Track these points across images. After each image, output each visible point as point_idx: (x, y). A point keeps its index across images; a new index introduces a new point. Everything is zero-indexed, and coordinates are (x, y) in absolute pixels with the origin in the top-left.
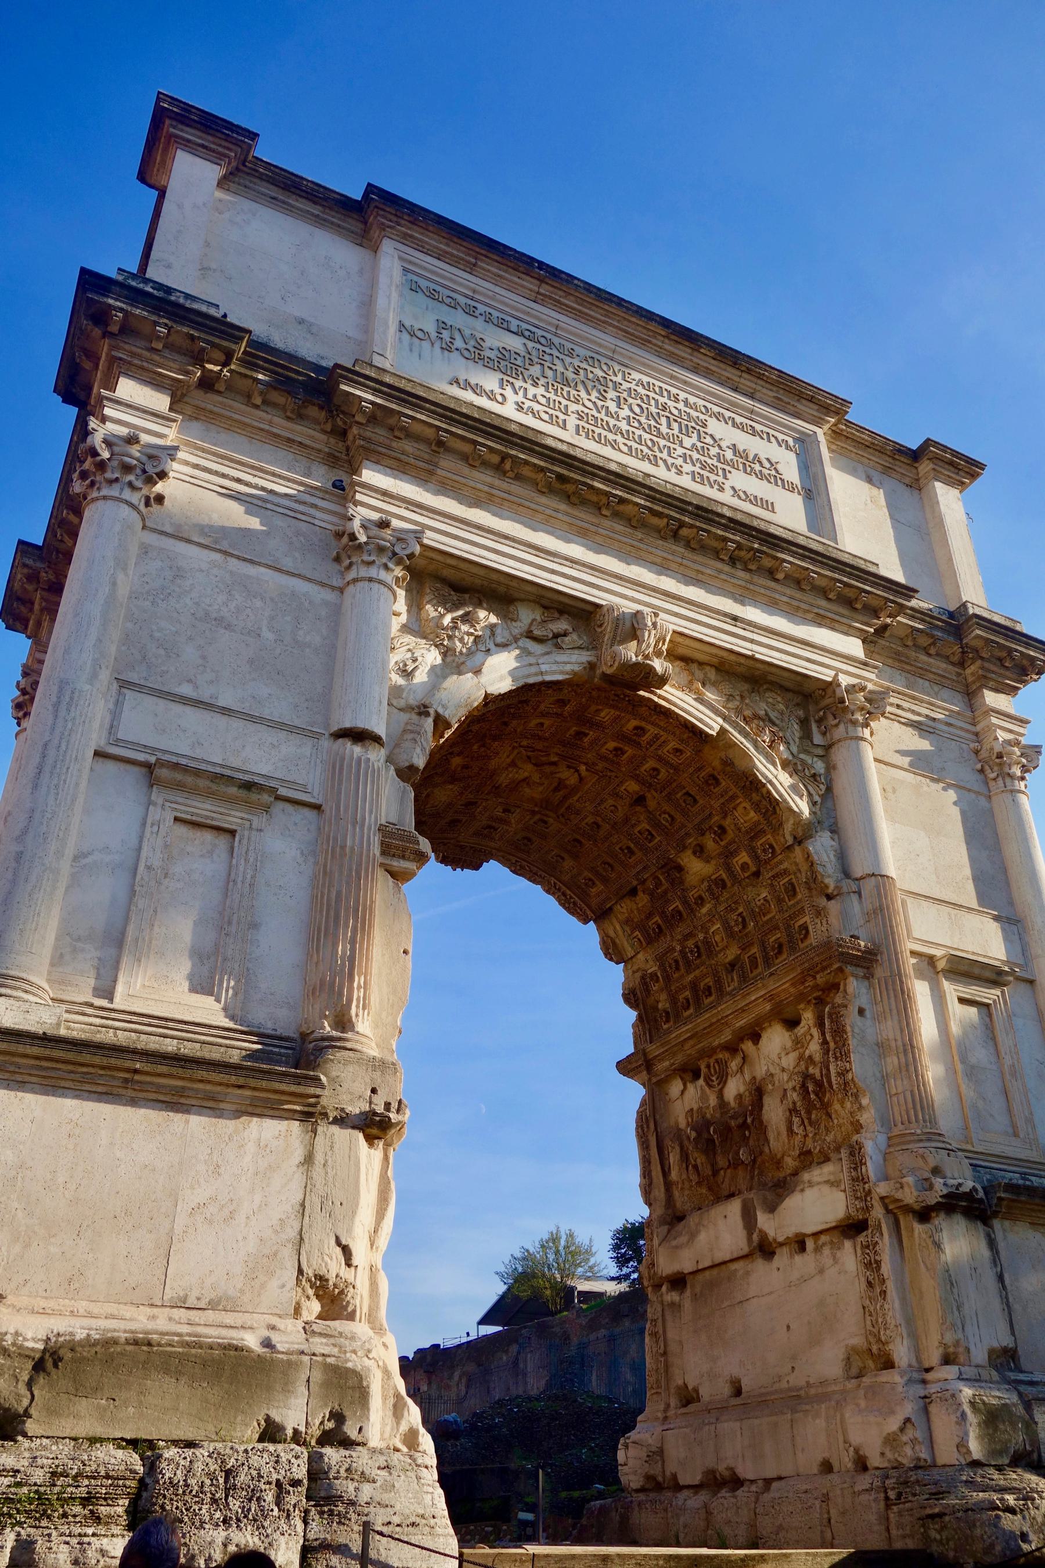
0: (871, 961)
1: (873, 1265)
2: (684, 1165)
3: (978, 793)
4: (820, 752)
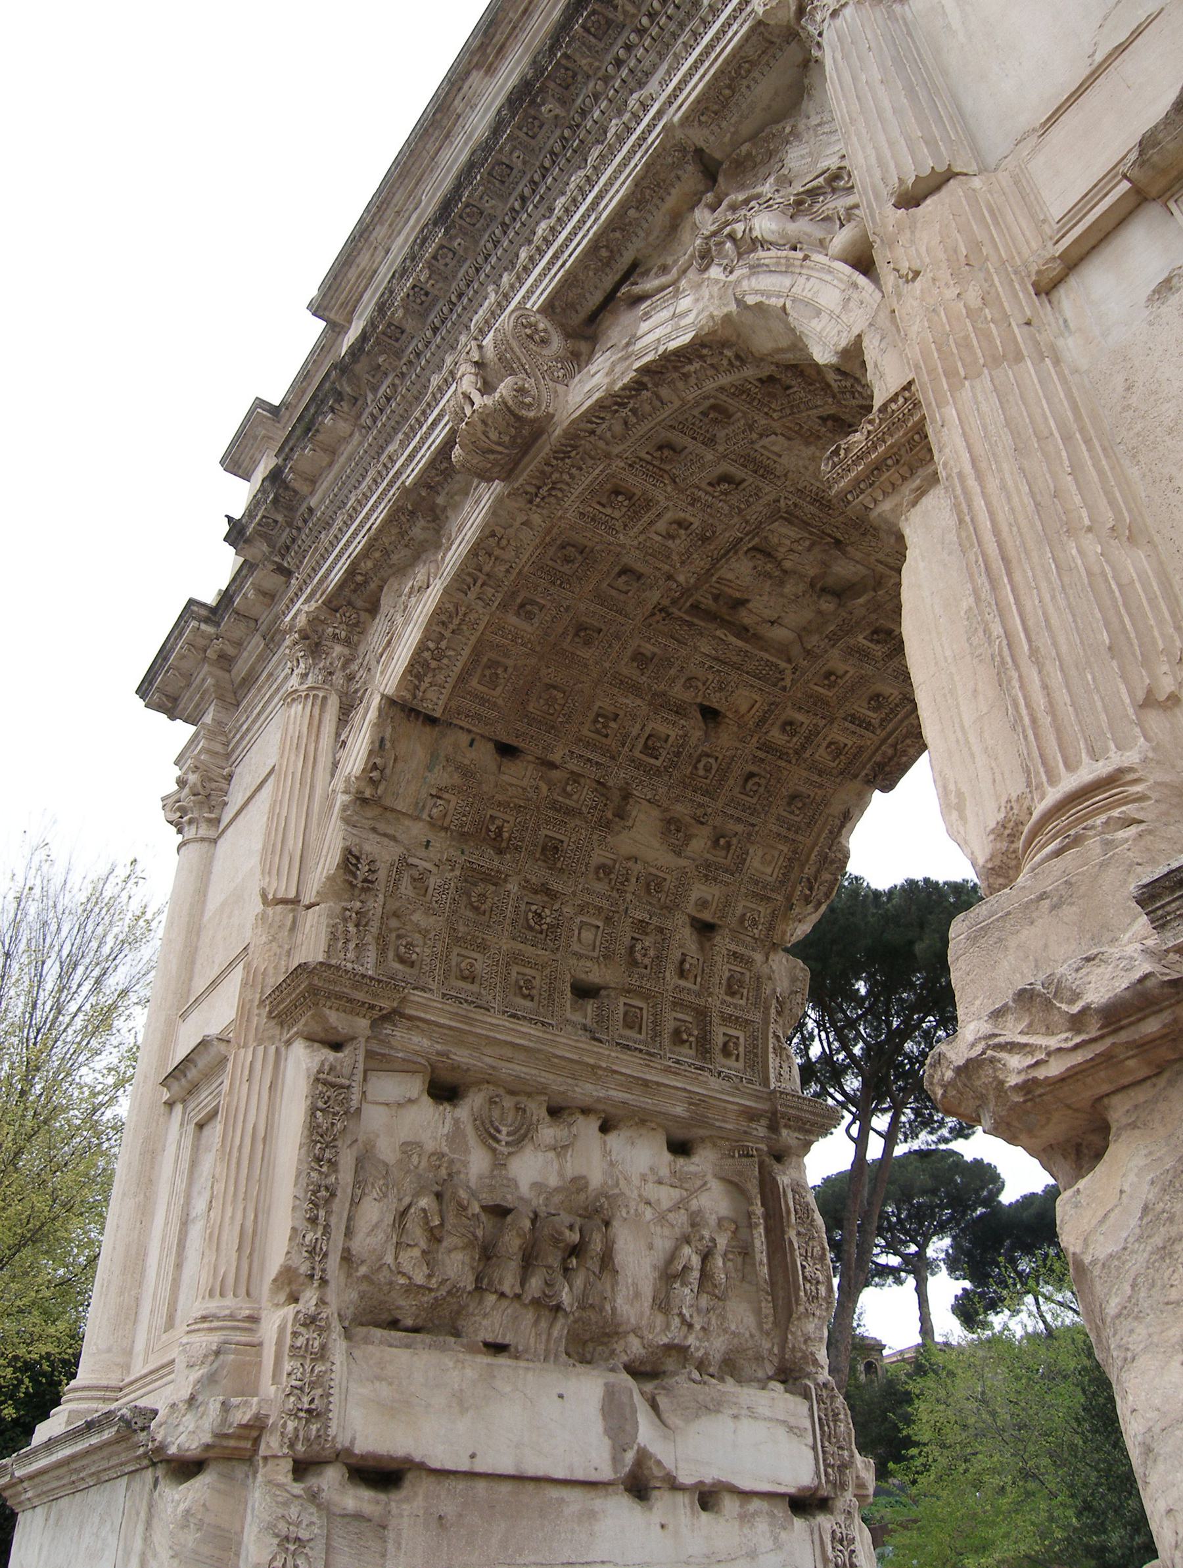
2: (395, 1240)
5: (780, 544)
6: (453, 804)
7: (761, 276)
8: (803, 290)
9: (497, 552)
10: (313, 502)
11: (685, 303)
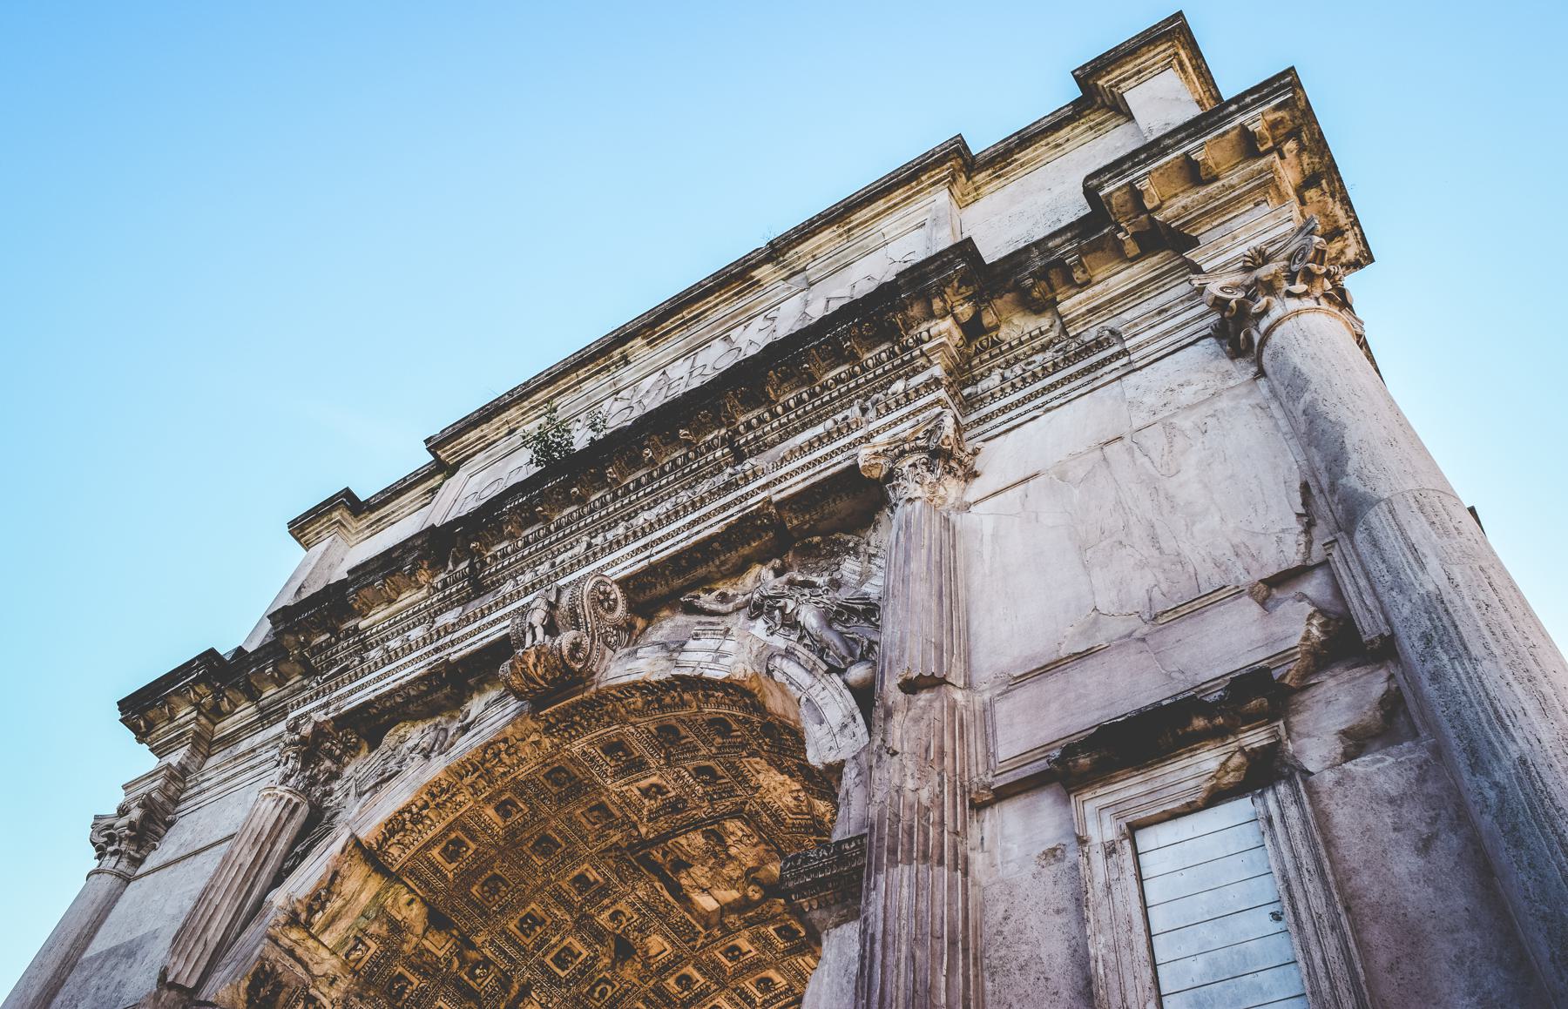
5: (732, 833)
6: (371, 951)
7: (792, 663)
8: (817, 696)
9: (503, 755)
10: (363, 624)
11: (729, 646)
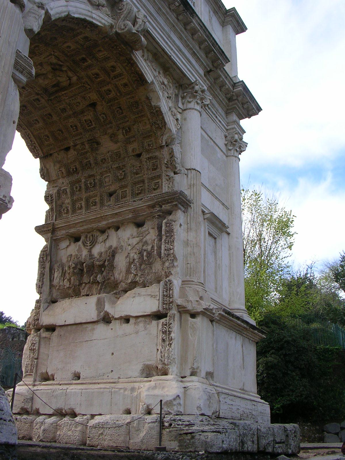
0: (187, 204)
1: (167, 332)
2: (62, 278)
3: (225, 154)
4: (180, 111)
